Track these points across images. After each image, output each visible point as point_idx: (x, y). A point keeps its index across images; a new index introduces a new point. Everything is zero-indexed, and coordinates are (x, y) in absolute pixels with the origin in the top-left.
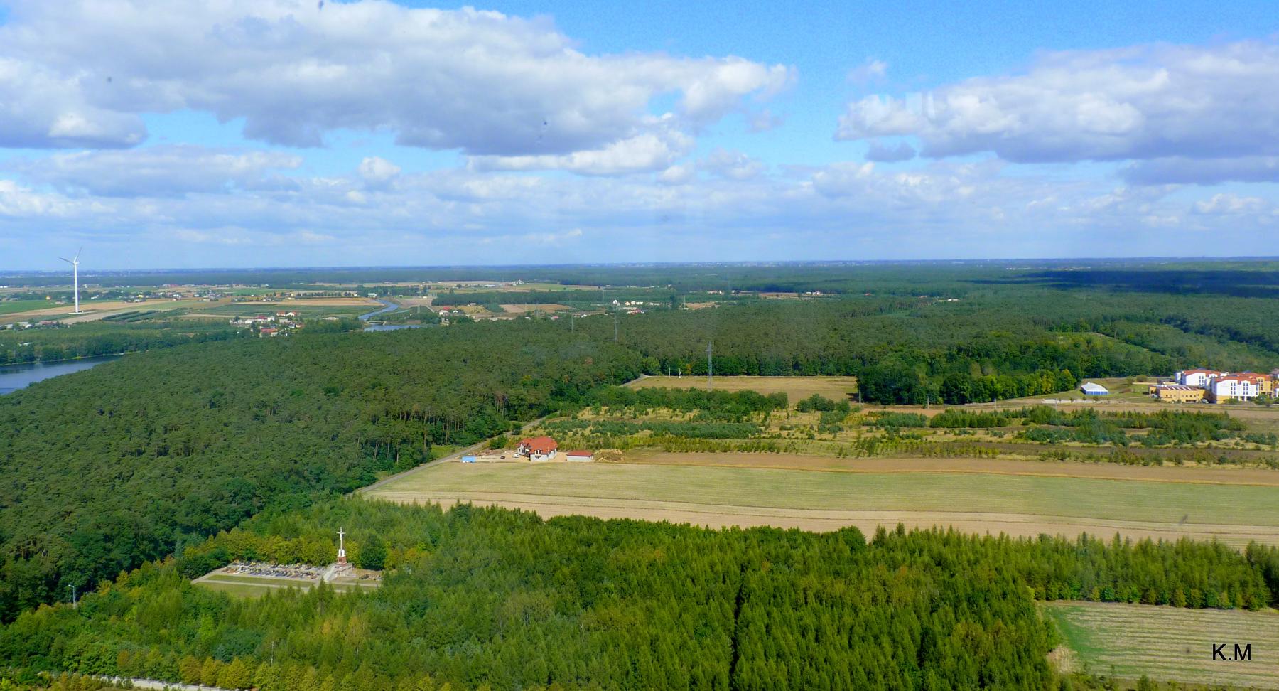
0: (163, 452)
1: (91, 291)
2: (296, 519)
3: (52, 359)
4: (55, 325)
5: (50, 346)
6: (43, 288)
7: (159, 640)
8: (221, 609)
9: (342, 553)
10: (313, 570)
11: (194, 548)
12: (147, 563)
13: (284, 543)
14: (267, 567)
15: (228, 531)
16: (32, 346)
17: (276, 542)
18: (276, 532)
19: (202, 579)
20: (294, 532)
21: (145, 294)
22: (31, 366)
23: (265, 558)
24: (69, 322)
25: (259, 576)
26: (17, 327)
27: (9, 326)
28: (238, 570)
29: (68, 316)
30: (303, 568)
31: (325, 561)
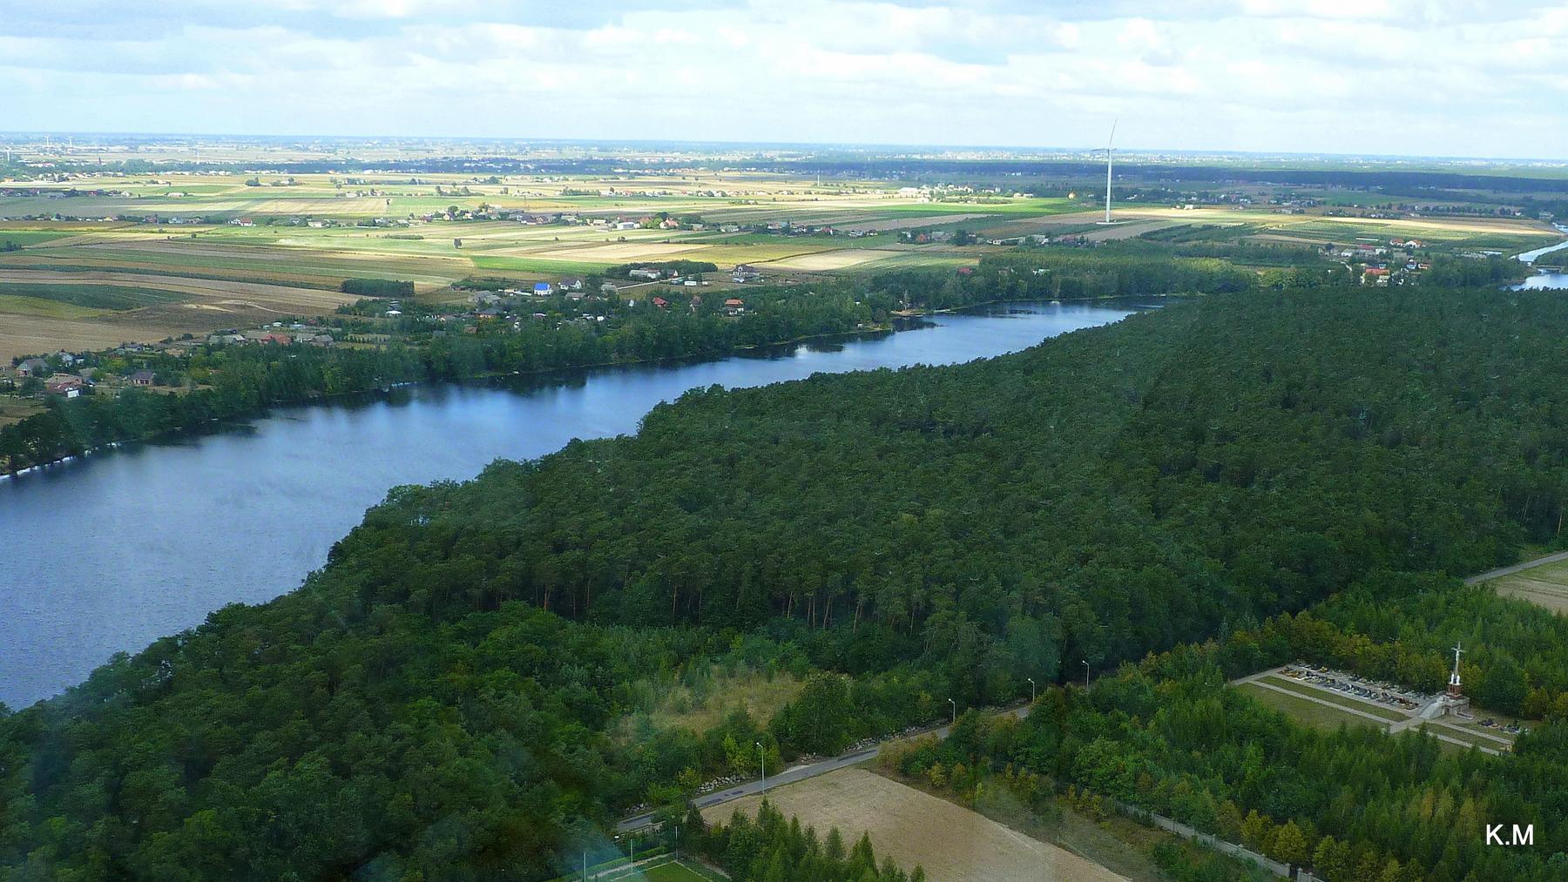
0: (1212, 475)
1: (1128, 186)
2: (1392, 610)
3: (1073, 296)
4: (1075, 240)
5: (1071, 277)
6: (1064, 179)
7: (1192, 768)
8: (1277, 739)
9: (1456, 679)
10: (1410, 696)
11: (1248, 635)
12: (1181, 646)
13: (1375, 648)
14: (1342, 678)
15: (1294, 614)
16: (1049, 276)
17: (1360, 644)
18: (1363, 629)
19: (1251, 680)
20: (1387, 633)
21: (1200, 196)
22: (1046, 303)
23: (1345, 665)
24: (1096, 237)
25: (1331, 690)
26: (1030, 241)
27: (1022, 240)
28: (1303, 676)
29: (1093, 228)
30: (1395, 692)
31: (1431, 686)
